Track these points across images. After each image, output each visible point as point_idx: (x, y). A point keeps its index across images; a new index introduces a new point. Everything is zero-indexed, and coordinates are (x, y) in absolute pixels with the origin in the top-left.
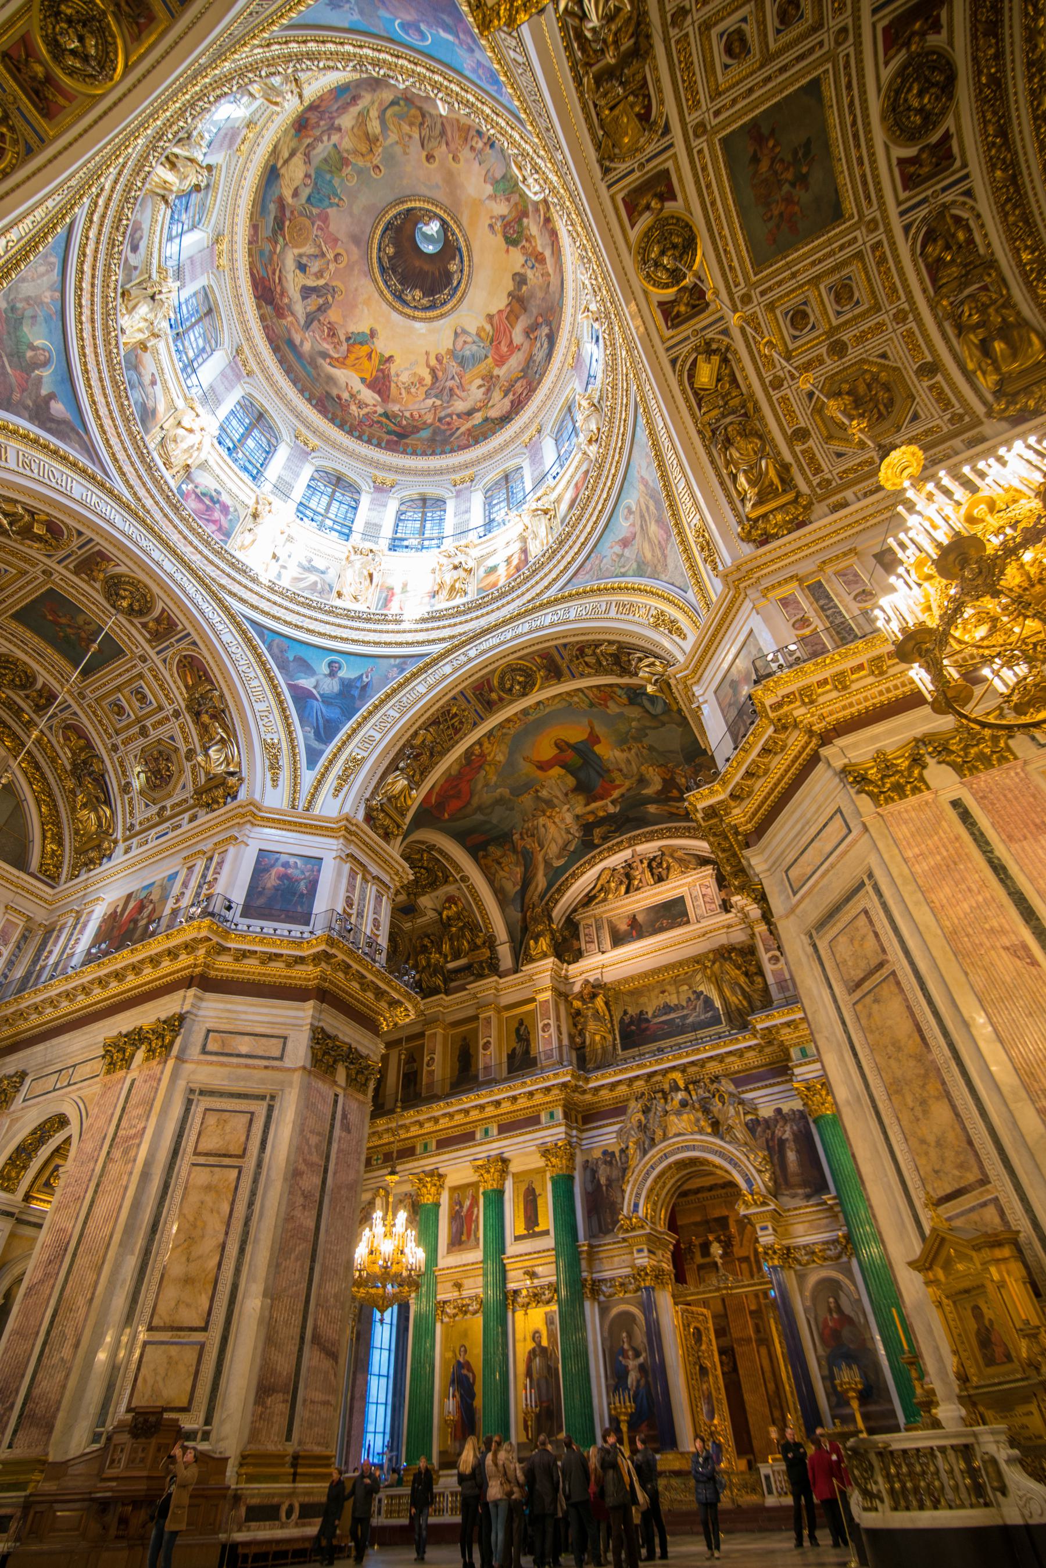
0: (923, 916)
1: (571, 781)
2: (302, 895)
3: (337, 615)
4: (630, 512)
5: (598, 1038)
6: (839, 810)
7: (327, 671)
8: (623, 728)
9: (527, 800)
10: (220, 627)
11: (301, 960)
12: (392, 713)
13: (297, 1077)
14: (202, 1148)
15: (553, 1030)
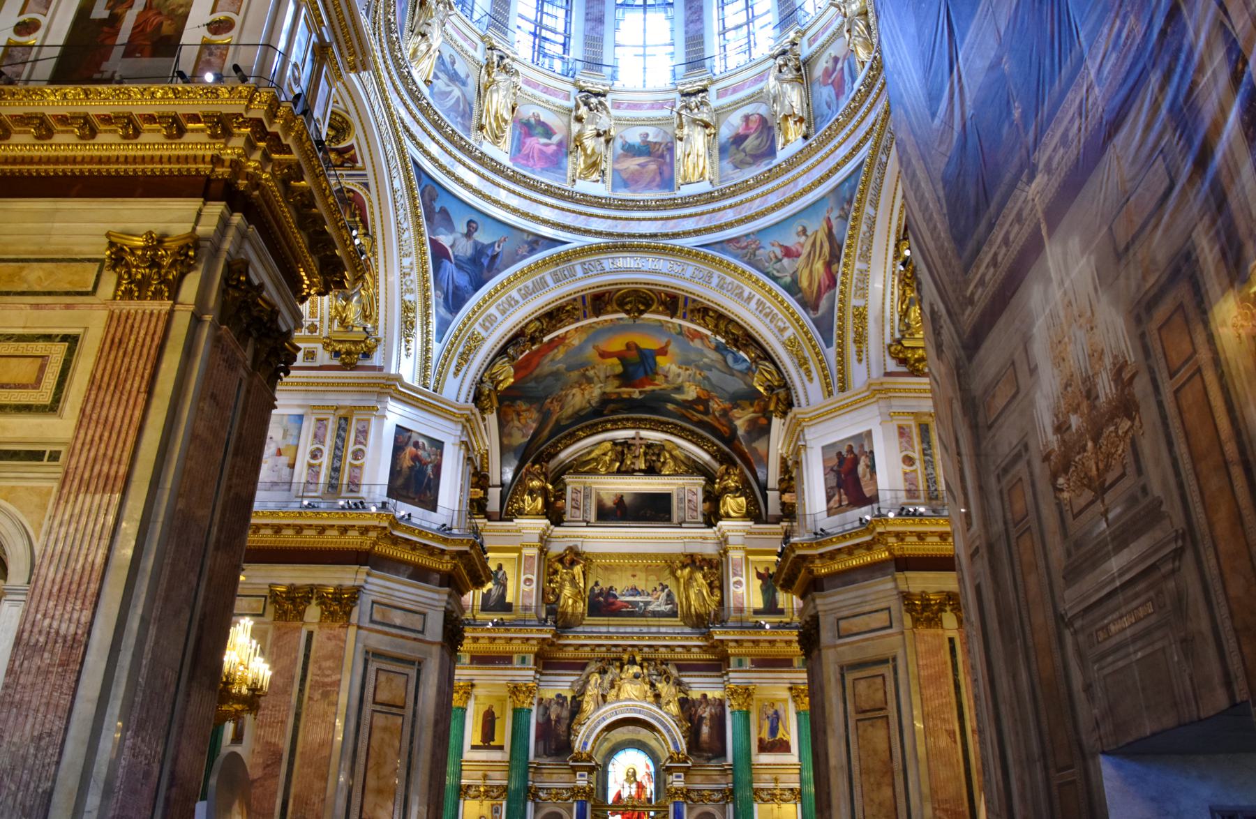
0: (916, 700)
1: (619, 369)
2: (429, 479)
3: (483, 164)
4: (804, 231)
5: (570, 601)
6: (889, 609)
7: (465, 231)
8: (693, 356)
9: (575, 375)
10: (394, 173)
11: (443, 552)
12: (518, 297)
13: (436, 650)
14: (380, 698)
15: (534, 585)
